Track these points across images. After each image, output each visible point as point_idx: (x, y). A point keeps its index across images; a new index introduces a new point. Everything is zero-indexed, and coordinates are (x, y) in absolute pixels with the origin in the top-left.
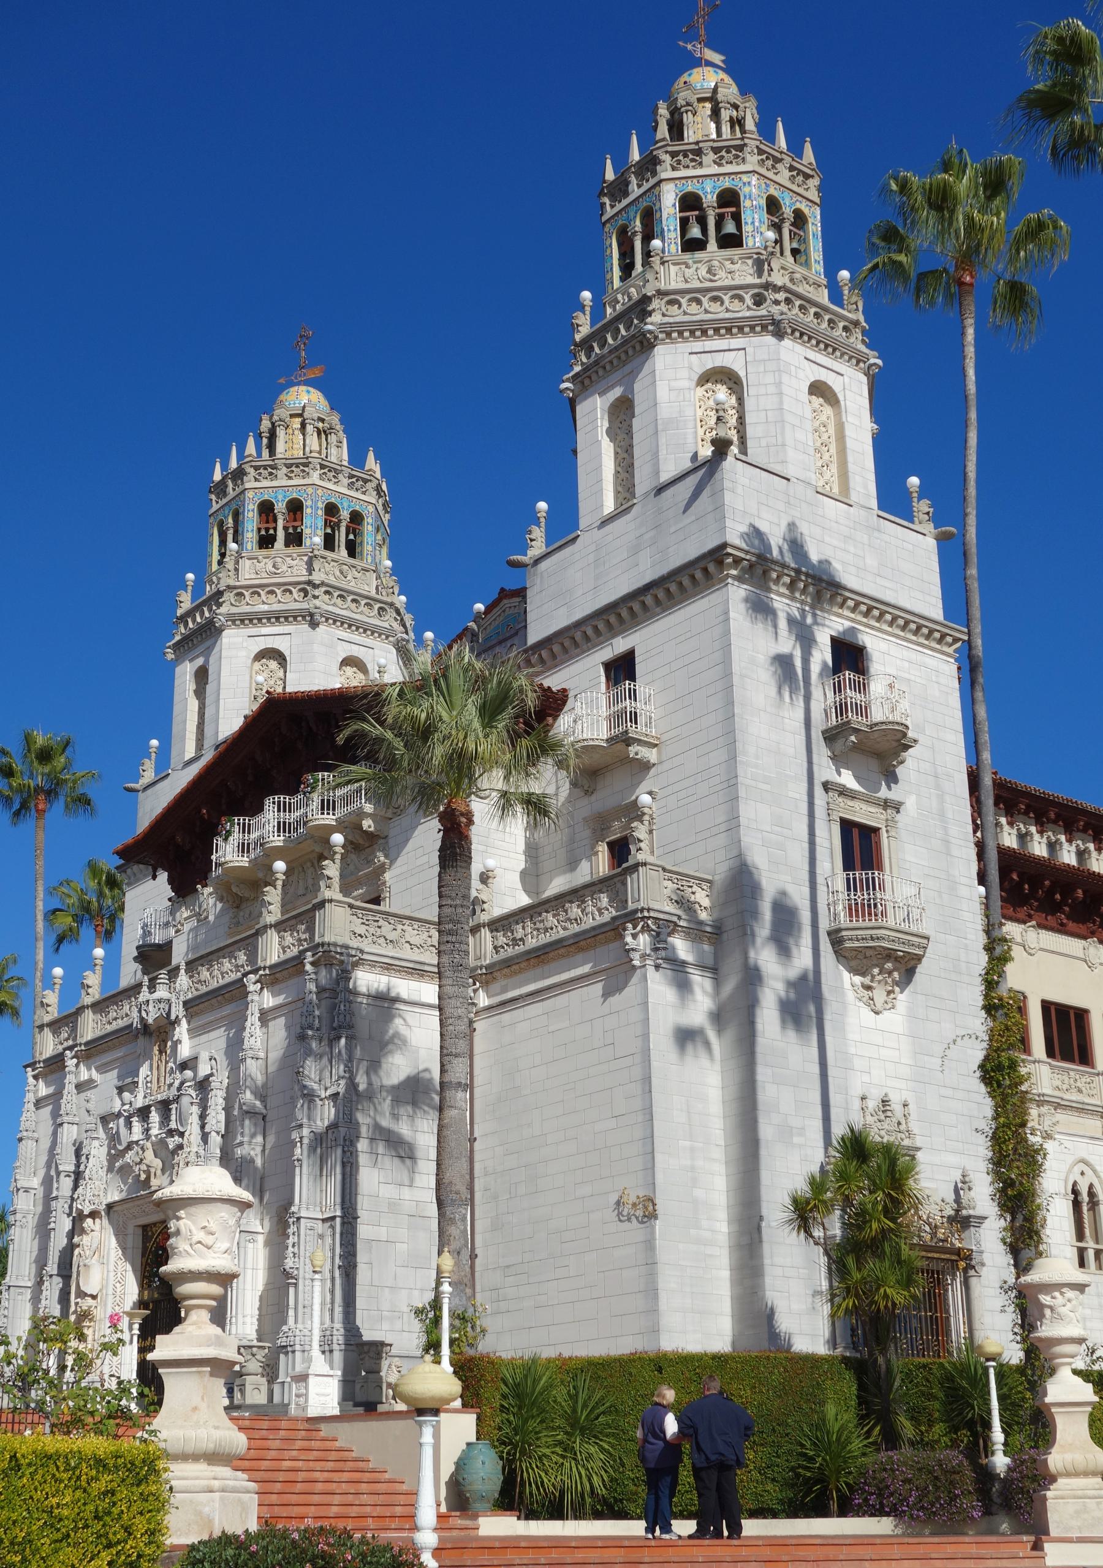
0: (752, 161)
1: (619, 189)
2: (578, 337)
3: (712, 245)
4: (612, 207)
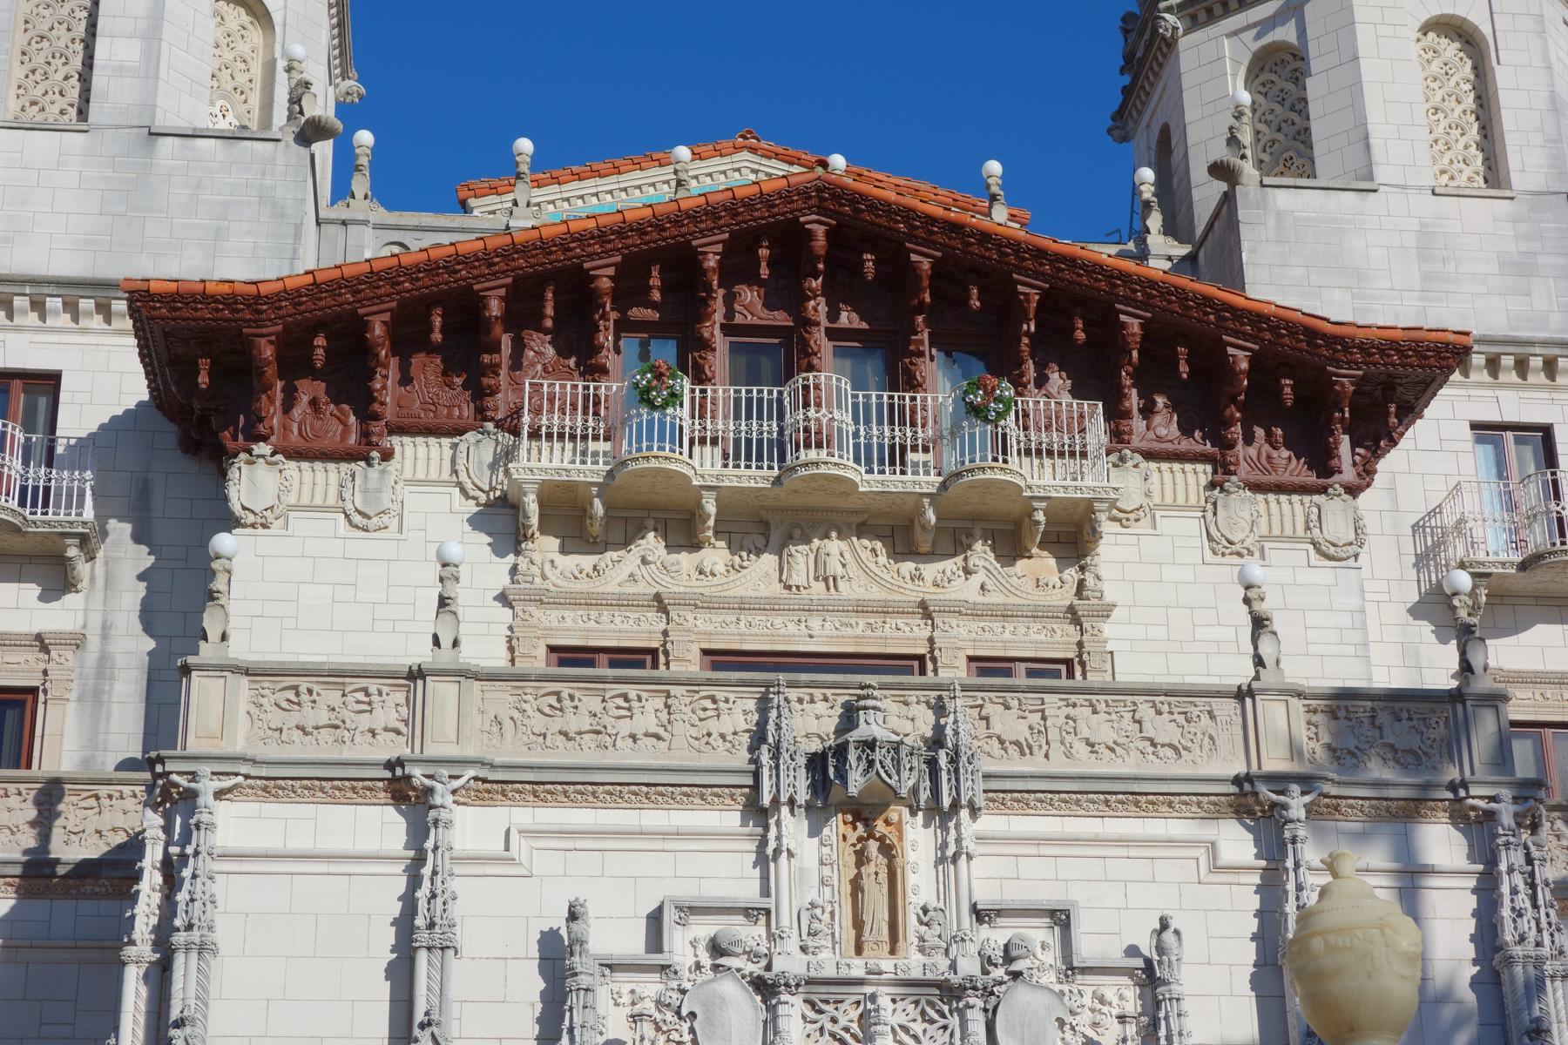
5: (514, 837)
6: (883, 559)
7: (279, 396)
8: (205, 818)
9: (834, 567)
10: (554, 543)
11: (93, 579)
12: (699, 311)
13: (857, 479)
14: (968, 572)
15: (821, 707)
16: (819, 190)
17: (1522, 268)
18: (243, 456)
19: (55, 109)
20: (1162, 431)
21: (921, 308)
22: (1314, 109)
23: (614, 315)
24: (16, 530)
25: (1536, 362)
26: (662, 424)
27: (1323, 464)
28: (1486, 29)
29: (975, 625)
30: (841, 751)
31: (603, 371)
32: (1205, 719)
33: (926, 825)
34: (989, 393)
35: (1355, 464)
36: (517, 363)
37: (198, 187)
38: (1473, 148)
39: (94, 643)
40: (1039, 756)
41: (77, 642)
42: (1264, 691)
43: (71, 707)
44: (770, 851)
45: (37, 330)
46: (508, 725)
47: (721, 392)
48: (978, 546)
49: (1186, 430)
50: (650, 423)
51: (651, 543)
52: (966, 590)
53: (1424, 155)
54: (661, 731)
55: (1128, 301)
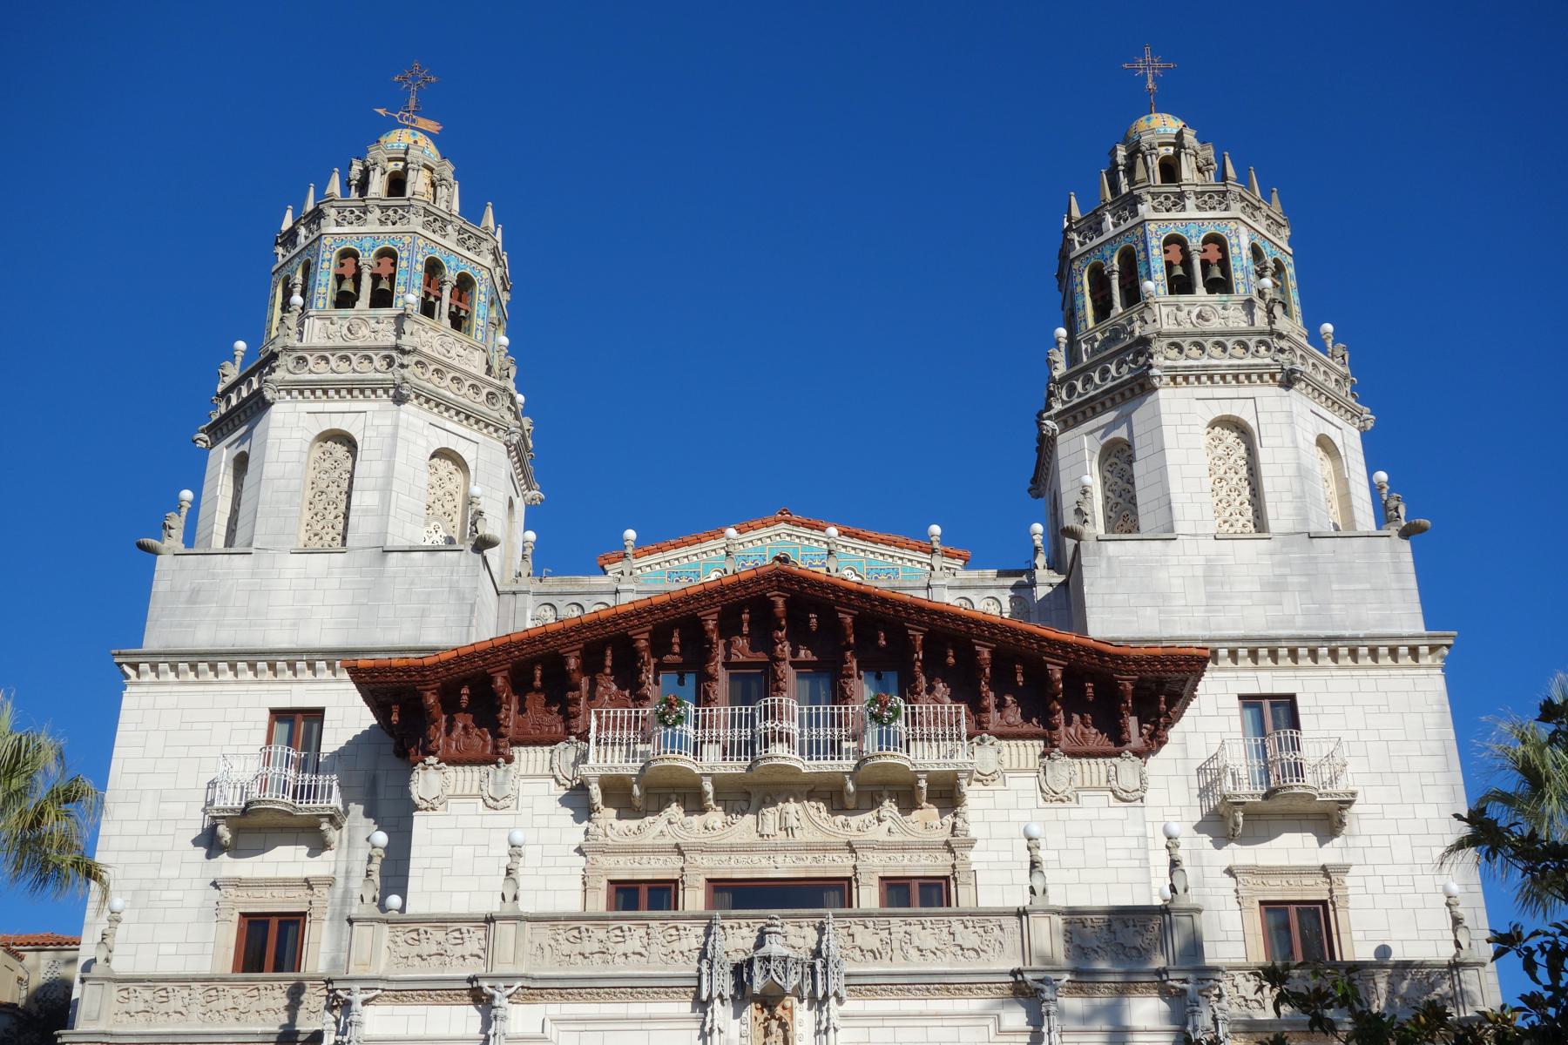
0: (1236, 209)
1: (1093, 225)
2: (1056, 374)
3: (1201, 290)
4: (1081, 244)
5: (548, 1024)
6: (824, 814)
7: (444, 725)
8: (355, 1018)
9: (792, 822)
10: (613, 812)
11: (341, 841)
12: (705, 656)
13: (800, 766)
14: (879, 820)
15: (745, 931)
16: (777, 576)
17: (1276, 586)
18: (420, 765)
19: (329, 538)
20: (1012, 720)
21: (848, 647)
22: (1138, 483)
23: (653, 661)
24: (290, 814)
25: (1283, 652)
26: (673, 736)
27: (1118, 738)
28: (1252, 424)
29: (884, 856)
30: (750, 962)
31: (646, 698)
32: (997, 930)
33: (810, 1009)
34: (883, 706)
35: (1141, 735)
36: (592, 696)
37: (412, 583)
38: (1246, 505)
39: (340, 882)
40: (886, 959)
41: (330, 882)
42: (1034, 911)
43: (326, 924)
44: (707, 1029)
45: (312, 682)
46: (547, 949)
47: (722, 711)
48: (887, 803)
49: (1026, 718)
50: (666, 735)
51: (675, 811)
52: (878, 833)
53: (1209, 513)
54: (643, 951)
55: (979, 637)
